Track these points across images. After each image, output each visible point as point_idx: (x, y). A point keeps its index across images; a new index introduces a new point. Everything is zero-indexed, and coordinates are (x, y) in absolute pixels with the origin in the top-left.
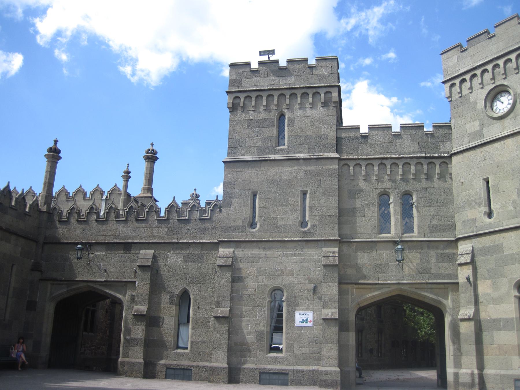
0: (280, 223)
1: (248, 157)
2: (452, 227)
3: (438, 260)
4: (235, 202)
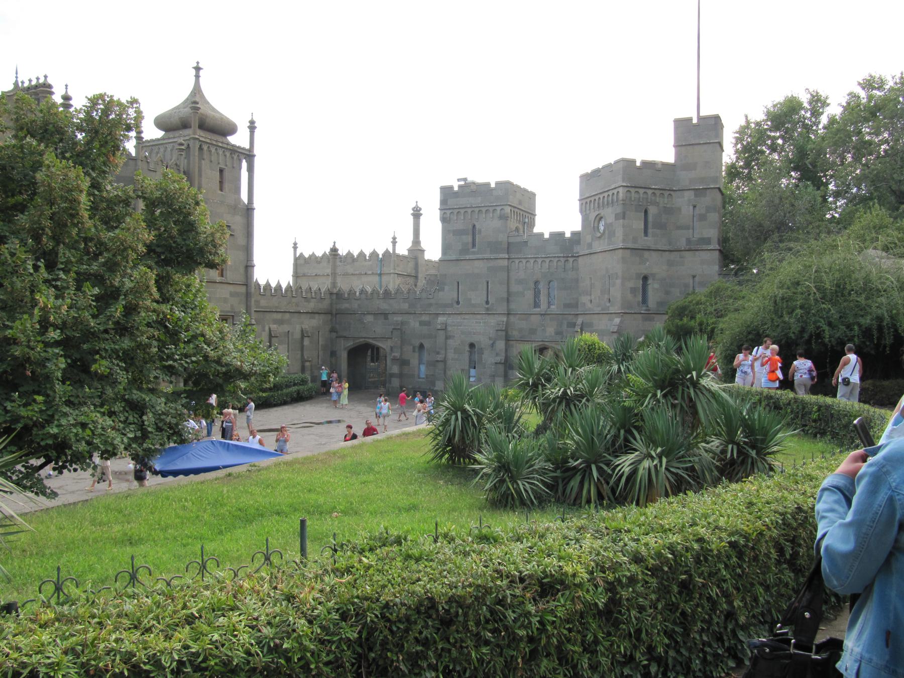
0: (473, 302)
1: (454, 257)
2: (576, 305)
3: (568, 327)
4: (446, 288)
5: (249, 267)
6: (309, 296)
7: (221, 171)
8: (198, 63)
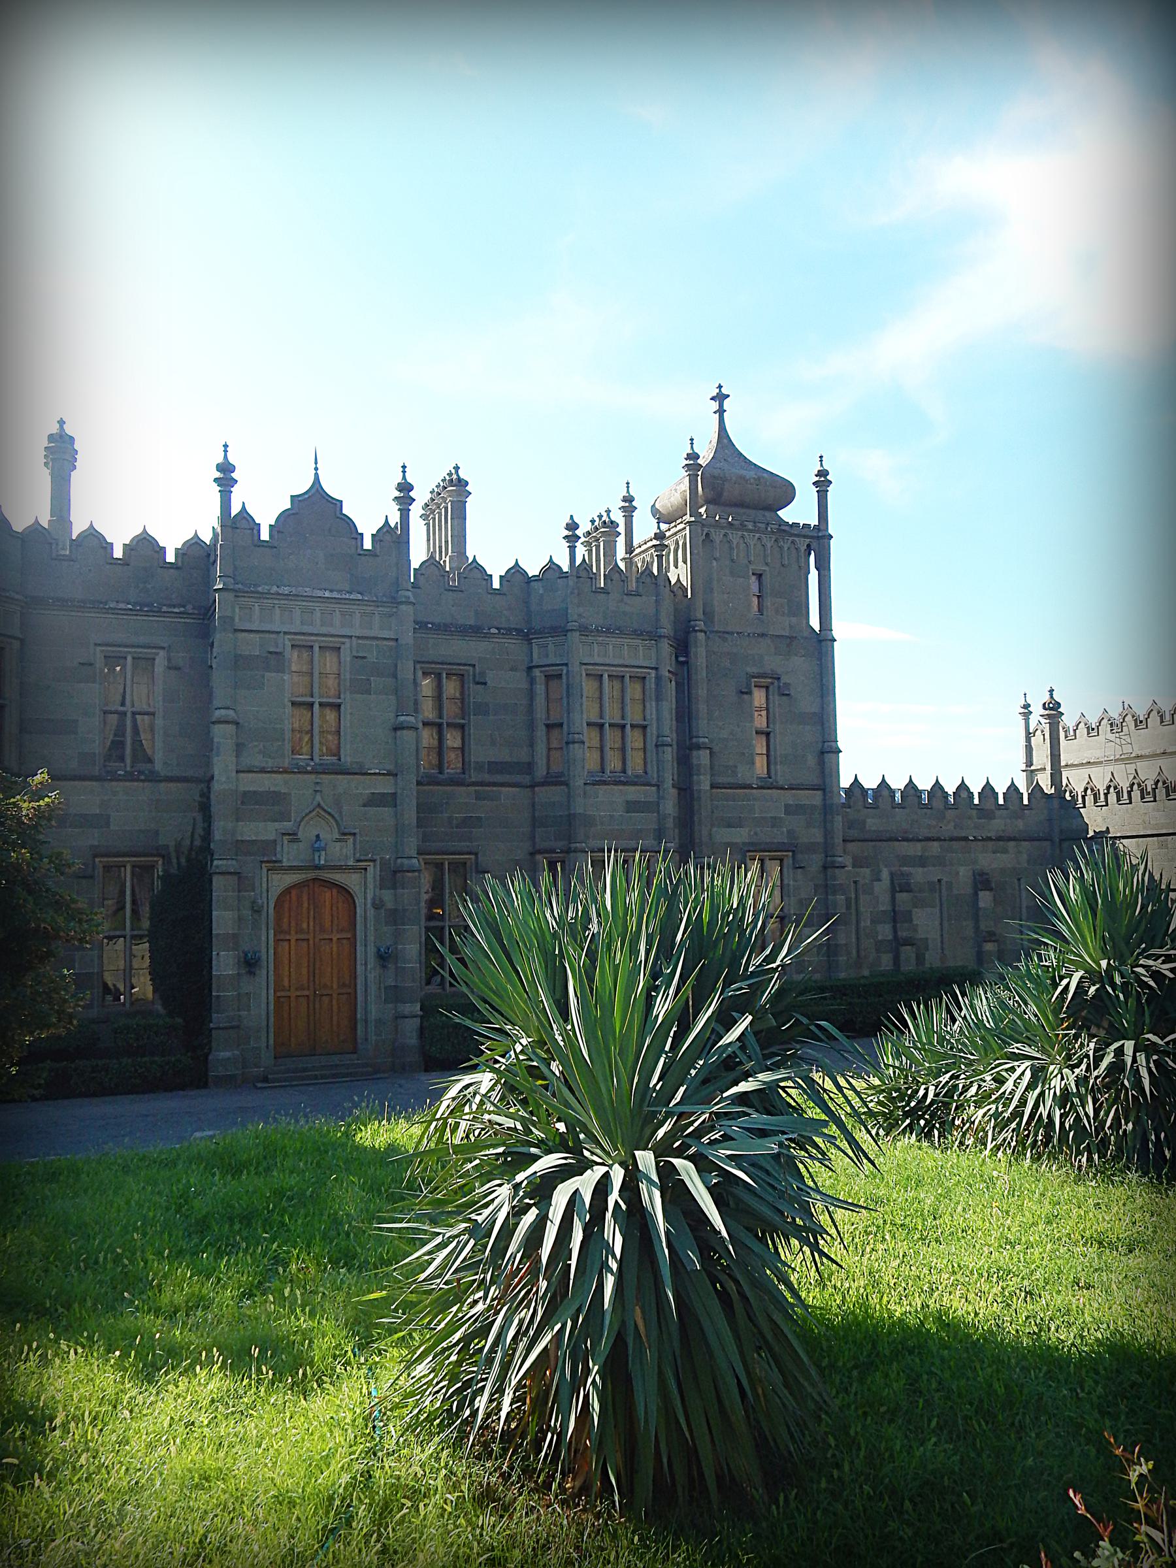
5: (828, 751)
6: (989, 805)
7: (759, 576)
8: (720, 387)
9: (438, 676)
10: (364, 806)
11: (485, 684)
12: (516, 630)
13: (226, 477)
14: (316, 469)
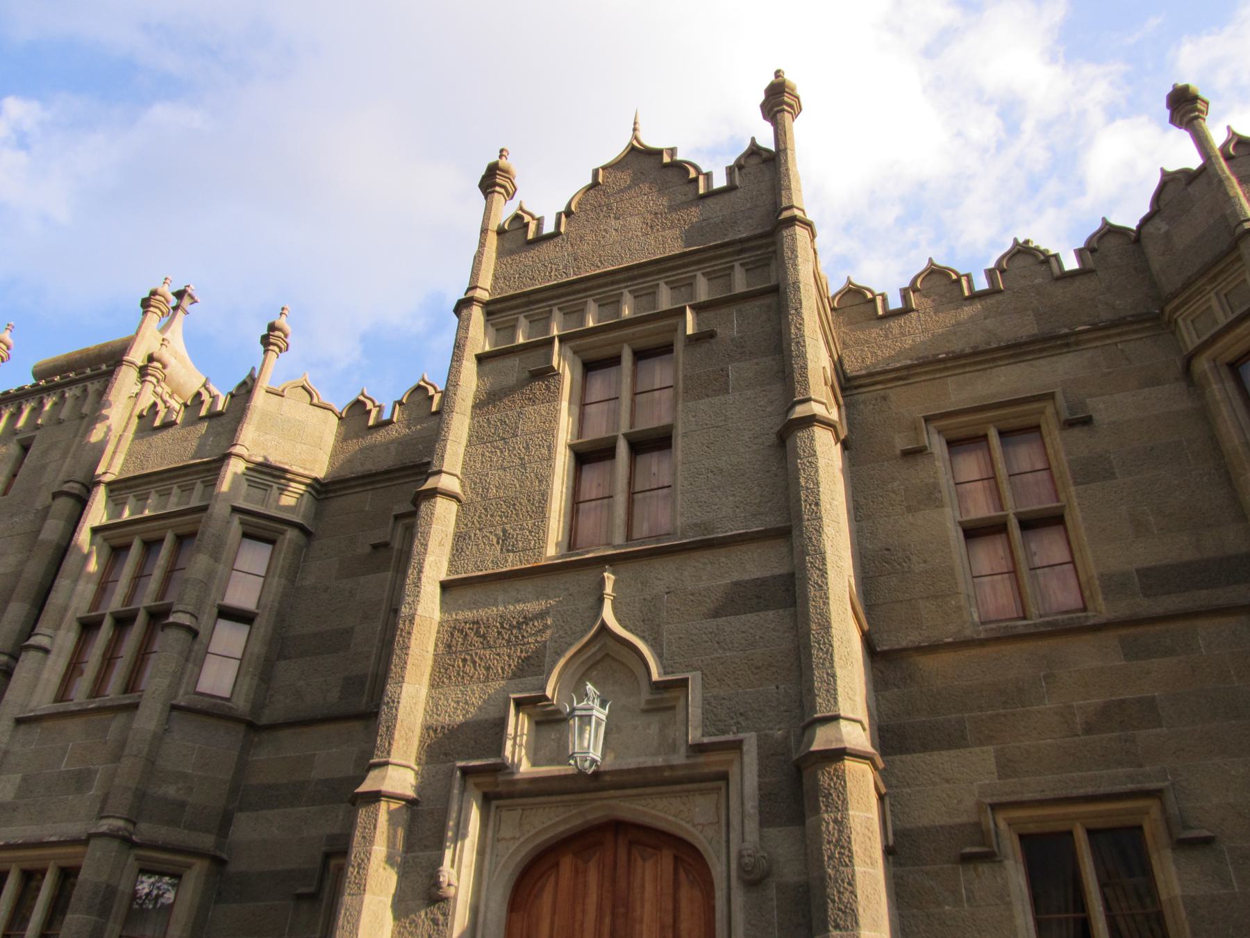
9: (980, 439)
10: (716, 614)
11: (1087, 421)
12: (1133, 316)
13: (493, 180)
14: (635, 130)
